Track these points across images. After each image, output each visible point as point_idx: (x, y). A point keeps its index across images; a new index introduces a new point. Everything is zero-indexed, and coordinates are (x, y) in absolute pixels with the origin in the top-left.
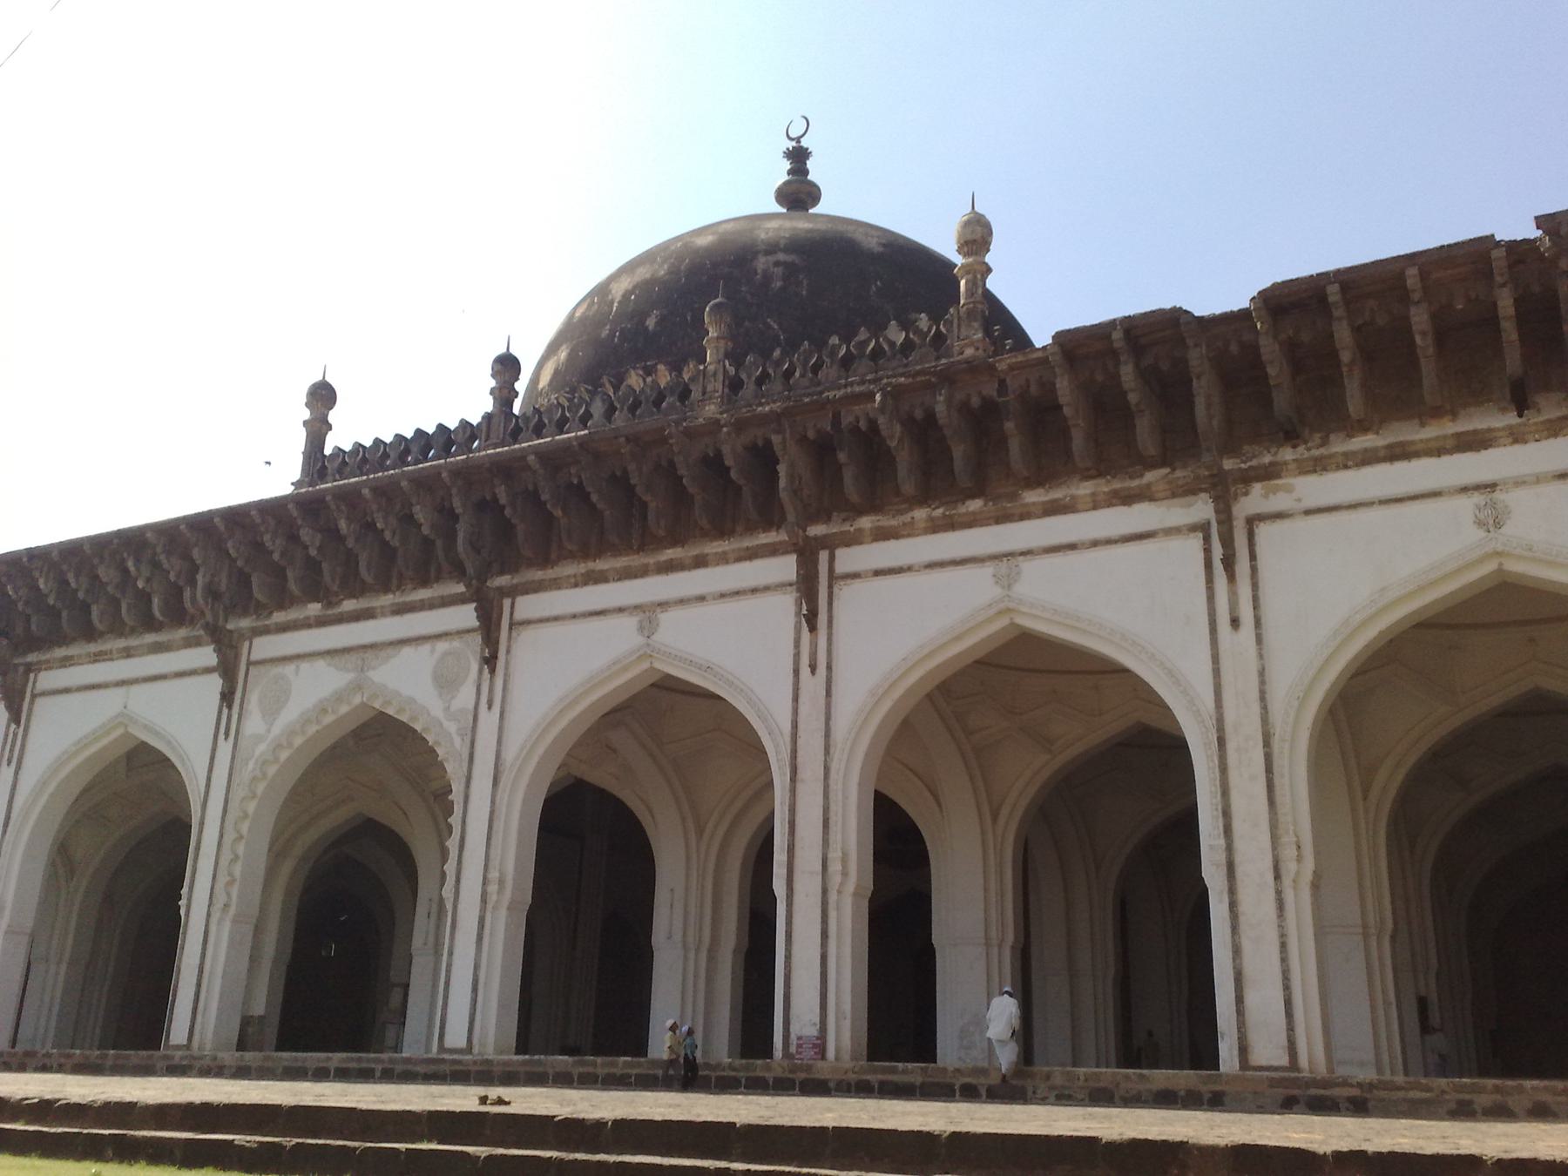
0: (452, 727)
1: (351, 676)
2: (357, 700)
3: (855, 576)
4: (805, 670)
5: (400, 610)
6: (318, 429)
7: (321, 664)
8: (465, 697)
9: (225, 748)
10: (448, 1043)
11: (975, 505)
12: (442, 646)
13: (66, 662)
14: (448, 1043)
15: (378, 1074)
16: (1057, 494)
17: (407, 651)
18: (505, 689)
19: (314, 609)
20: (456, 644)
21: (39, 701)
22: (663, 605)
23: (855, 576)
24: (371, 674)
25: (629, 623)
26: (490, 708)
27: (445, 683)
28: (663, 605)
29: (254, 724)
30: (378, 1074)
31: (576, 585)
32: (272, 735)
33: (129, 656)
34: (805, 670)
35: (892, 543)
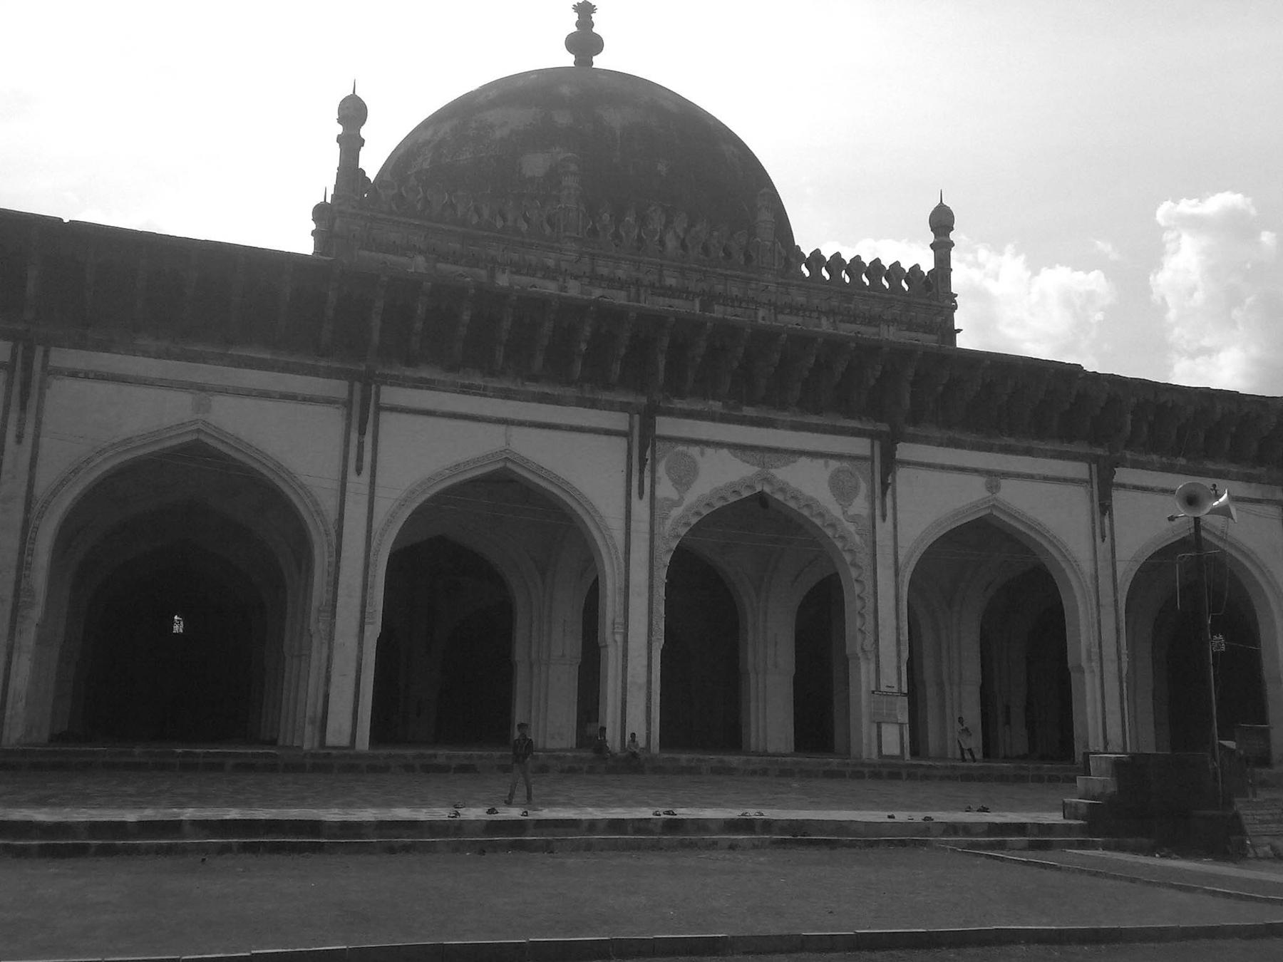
0: (852, 528)
1: (757, 469)
2: (758, 489)
3: (1123, 486)
4: (1099, 540)
5: (796, 427)
6: (351, 144)
7: (725, 452)
8: (860, 505)
9: (641, 509)
10: (885, 751)
11: (1182, 461)
12: (834, 464)
13: (428, 384)
14: (885, 751)
15: (904, 776)
16: (1220, 467)
17: (803, 461)
18: (894, 508)
19: (716, 406)
20: (846, 465)
21: (384, 416)
22: (1006, 475)
23: (1123, 486)
24: (773, 471)
25: (979, 482)
26: (884, 520)
27: (843, 492)
28: (1006, 475)
29: (666, 489)
30: (904, 776)
31: (941, 445)
32: (686, 502)
33: (507, 398)
34: (1099, 540)
35: (1139, 471)
